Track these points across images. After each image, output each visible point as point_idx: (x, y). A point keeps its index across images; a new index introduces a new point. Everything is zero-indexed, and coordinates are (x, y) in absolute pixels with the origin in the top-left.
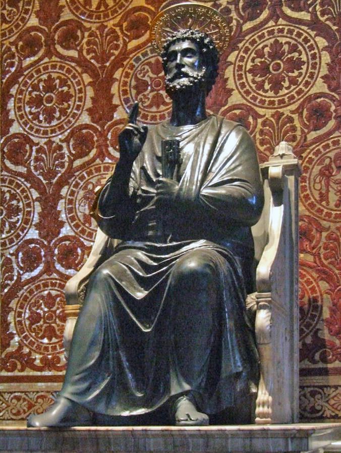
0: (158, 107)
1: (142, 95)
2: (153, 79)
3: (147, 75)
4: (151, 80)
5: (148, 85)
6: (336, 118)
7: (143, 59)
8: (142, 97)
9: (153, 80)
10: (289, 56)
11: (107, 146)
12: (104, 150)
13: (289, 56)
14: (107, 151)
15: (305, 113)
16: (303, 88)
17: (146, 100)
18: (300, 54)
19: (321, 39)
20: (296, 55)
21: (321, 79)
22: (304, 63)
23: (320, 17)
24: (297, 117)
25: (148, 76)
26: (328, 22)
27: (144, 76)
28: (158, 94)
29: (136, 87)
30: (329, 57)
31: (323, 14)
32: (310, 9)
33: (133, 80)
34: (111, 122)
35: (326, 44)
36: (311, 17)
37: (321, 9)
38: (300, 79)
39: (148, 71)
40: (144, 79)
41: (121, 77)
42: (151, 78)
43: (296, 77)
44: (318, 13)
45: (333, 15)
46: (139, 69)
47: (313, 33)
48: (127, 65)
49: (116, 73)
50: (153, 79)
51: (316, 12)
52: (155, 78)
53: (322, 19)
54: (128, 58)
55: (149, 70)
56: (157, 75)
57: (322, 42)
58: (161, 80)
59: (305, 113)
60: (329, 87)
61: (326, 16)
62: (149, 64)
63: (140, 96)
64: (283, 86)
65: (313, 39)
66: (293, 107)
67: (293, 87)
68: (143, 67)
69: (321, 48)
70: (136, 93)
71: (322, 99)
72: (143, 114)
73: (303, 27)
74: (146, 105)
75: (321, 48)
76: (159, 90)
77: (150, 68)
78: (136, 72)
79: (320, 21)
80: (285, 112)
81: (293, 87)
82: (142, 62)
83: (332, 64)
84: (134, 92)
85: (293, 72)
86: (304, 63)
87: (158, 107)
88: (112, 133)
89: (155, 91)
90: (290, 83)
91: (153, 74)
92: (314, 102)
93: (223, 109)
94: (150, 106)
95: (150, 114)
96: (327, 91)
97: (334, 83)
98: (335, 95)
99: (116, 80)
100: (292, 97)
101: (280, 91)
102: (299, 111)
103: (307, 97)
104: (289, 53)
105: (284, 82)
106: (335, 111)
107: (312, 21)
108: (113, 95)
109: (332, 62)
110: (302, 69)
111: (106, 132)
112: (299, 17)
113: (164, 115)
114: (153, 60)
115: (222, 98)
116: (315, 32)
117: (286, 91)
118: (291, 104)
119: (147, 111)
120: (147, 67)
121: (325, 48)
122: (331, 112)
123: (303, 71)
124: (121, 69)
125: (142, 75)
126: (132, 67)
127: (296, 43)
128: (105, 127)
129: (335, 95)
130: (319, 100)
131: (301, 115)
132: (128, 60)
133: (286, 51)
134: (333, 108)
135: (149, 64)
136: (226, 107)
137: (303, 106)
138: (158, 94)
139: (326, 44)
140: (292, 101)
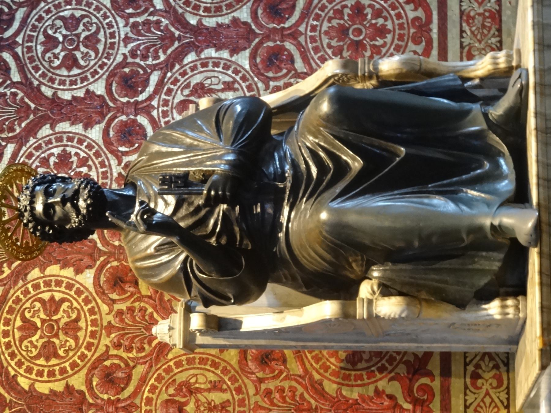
0: (80, 329)
1: (60, 349)
2: (43, 335)
3: (35, 343)
4: (43, 338)
5: (49, 342)
6: (136, 115)
7: (14, 348)
8: (62, 349)
9: (44, 334)
10: (52, 167)
11: (118, 400)
12: (123, 405)
13: (52, 167)
14: (125, 400)
15: (123, 149)
16: (94, 151)
17: (68, 344)
18: (52, 154)
19: (40, 132)
20: (52, 160)
21: (87, 131)
22: (64, 151)
23: (15, 133)
24: (127, 157)
25: (37, 341)
26: (23, 125)
27: (36, 347)
28: (63, 329)
29: (47, 359)
30: (64, 123)
31: (11, 129)
32: (4, 144)
33: (38, 362)
34: (87, 394)
35: (48, 126)
36: (12, 143)
37: (6, 132)
38: (82, 154)
39: (31, 342)
40: (39, 347)
41: (30, 379)
42: (41, 337)
43: (79, 159)
44: (10, 135)
45: (15, 120)
46: (24, 353)
47: (32, 141)
48: (15, 371)
49: (22, 385)
50: (43, 335)
51: (8, 137)
52: (42, 332)
53: (18, 130)
54: (7, 367)
55: (29, 339)
56: (39, 329)
57: (45, 131)
58: (46, 324)
59: (123, 149)
60: (99, 123)
61: (15, 127)
62: (21, 341)
63: (61, 352)
64: (86, 174)
65: (39, 140)
66: (114, 162)
67: (90, 163)
68: (24, 348)
69: (51, 132)
70: (56, 358)
71: (111, 130)
72: (85, 350)
73: (22, 152)
74: (74, 346)
75: (51, 132)
76: (58, 326)
77: (27, 339)
78: (28, 358)
79: (19, 133)
80: (119, 171)
81: (90, 163)
82: (17, 349)
83: (73, 120)
84: (54, 361)
85: (72, 162)
86: (64, 151)
87: (80, 329)
88: (102, 393)
89: (58, 332)
90: (84, 166)
91: (35, 334)
92: (112, 139)
93: (99, 245)
94: (76, 339)
95: (88, 339)
96: (103, 125)
97: (96, 118)
98: (109, 116)
99: (32, 386)
100: (103, 164)
101: (91, 177)
102: (119, 156)
103: (105, 147)
104: (48, 166)
105: (82, 172)
106: (127, 115)
107: (17, 143)
108: (51, 391)
109: (70, 120)
110: (70, 152)
111: (99, 401)
112: (9, 156)
113: (92, 321)
114: (17, 335)
115: (86, 246)
116: (31, 138)
117: (94, 169)
118: (110, 165)
119: (83, 343)
120: (25, 343)
121: (52, 127)
122: (129, 119)
123: (73, 151)
124: (20, 380)
125: (33, 350)
126: (20, 364)
127: (38, 160)
128: (91, 401)
129: (109, 116)
130: (112, 133)
131: (126, 154)
132: (10, 369)
133: (45, 170)
134: (124, 118)
135: (21, 340)
136: (98, 241)
137: (114, 150)
138: (63, 329)
139: (48, 126)
140: (107, 163)
